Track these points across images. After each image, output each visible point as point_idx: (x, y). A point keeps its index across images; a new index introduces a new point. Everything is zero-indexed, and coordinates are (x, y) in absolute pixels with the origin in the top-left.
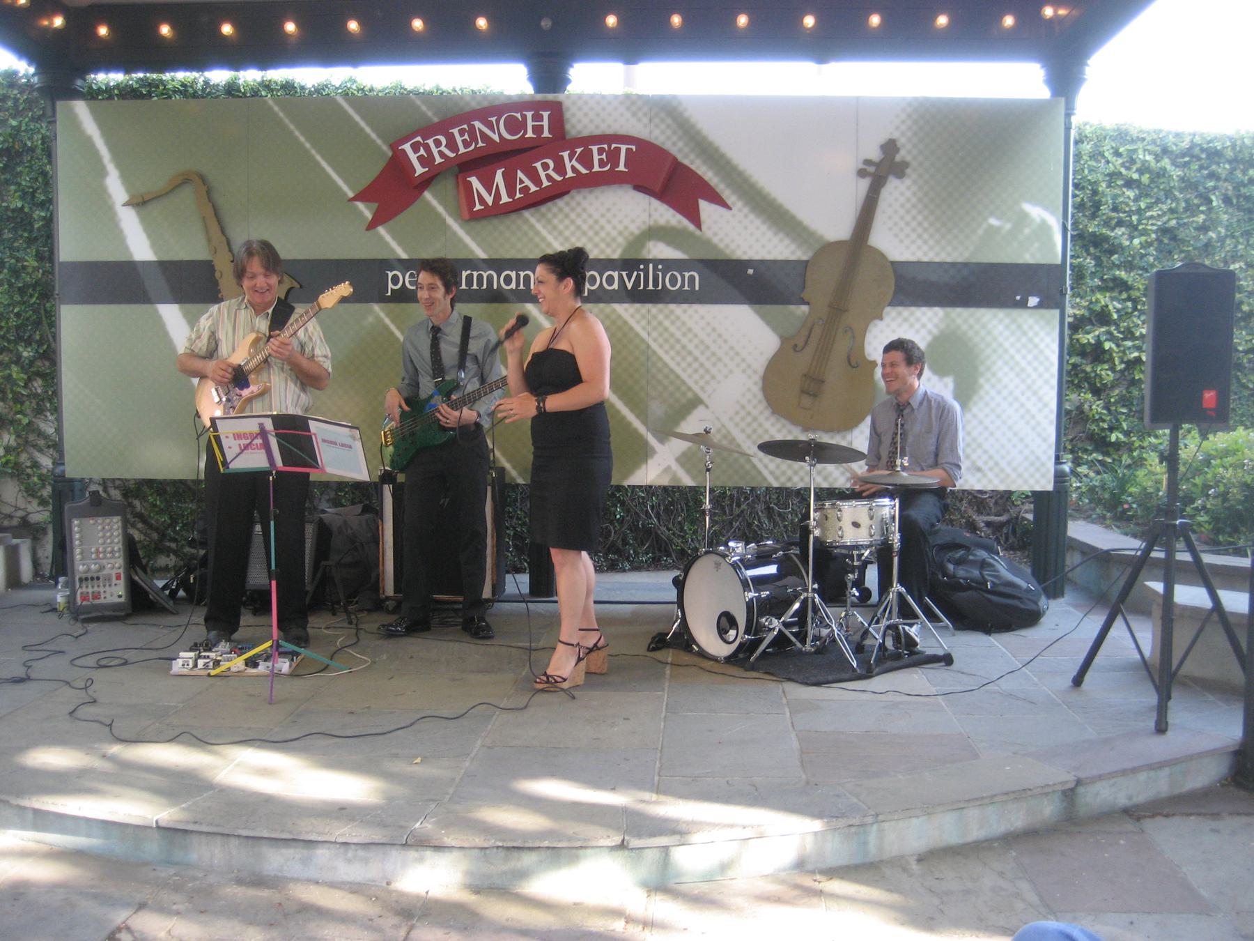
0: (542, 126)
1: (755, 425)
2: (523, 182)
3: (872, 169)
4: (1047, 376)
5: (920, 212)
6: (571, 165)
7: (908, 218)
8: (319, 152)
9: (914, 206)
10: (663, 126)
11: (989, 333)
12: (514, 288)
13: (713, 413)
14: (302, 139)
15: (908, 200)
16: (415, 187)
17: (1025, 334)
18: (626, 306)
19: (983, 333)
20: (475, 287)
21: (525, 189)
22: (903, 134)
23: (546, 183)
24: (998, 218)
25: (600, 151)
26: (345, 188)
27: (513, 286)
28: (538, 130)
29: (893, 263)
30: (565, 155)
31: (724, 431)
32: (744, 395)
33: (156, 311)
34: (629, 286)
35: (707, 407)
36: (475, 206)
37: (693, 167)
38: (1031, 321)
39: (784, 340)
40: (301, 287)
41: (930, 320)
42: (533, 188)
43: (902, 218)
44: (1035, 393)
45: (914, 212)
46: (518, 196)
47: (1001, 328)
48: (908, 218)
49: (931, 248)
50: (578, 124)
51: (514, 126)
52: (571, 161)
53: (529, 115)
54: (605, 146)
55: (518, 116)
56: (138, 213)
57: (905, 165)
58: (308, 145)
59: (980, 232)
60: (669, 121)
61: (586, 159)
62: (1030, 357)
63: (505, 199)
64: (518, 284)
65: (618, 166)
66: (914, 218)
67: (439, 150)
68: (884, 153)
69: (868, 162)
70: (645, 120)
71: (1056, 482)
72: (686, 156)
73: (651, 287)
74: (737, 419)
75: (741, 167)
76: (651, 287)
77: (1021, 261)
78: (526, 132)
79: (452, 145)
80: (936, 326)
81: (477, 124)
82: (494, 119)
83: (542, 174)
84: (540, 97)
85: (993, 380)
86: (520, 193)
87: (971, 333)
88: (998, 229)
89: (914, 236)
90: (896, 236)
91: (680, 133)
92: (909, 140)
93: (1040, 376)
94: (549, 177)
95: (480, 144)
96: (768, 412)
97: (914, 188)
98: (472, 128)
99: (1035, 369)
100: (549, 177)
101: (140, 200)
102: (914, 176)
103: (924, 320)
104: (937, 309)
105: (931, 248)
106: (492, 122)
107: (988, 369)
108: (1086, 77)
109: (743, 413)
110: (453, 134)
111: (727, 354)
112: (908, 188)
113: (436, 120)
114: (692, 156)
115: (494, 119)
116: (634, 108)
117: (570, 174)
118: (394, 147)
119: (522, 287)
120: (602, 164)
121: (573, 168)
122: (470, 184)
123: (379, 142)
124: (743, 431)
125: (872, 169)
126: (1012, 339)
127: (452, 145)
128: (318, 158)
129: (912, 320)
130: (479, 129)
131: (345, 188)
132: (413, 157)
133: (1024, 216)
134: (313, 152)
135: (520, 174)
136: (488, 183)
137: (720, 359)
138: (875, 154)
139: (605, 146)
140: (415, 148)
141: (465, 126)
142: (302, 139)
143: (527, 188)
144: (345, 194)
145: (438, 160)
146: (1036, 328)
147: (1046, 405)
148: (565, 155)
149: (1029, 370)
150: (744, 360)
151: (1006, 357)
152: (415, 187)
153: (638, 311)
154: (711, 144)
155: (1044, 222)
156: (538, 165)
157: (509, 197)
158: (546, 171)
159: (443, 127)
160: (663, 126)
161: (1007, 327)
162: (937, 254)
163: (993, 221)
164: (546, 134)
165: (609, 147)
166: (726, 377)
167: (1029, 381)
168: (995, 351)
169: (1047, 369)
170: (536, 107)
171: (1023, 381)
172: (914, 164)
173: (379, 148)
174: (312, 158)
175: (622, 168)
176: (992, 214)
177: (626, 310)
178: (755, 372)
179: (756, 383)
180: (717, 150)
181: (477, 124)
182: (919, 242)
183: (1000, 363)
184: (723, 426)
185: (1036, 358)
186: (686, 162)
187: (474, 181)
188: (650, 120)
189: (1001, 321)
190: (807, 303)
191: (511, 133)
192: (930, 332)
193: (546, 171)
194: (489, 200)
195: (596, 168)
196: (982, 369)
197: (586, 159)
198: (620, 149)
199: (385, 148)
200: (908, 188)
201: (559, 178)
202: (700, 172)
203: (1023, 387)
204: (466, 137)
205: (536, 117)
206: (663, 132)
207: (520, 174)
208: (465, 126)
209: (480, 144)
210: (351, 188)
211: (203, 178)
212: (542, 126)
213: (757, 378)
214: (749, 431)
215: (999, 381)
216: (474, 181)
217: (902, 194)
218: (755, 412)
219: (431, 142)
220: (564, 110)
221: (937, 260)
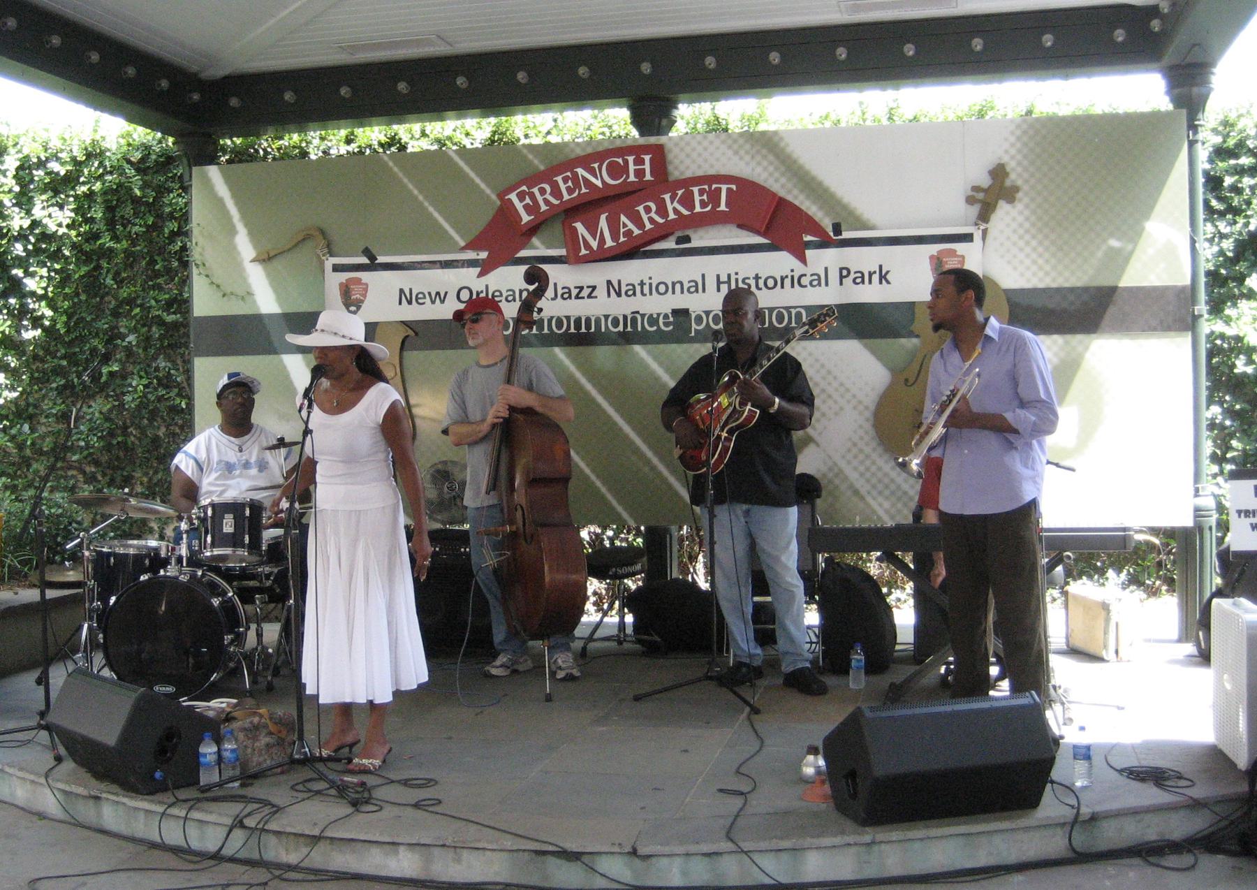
0: (644, 169)
1: (868, 463)
2: (627, 226)
3: (981, 196)
5: (1034, 237)
6: (673, 207)
7: (1021, 243)
9: (1027, 231)
10: (765, 163)
12: (622, 330)
13: (824, 451)
15: (1021, 225)
16: (523, 234)
20: (583, 330)
21: (628, 233)
22: (1013, 158)
23: (648, 226)
24: (1119, 239)
25: (701, 192)
28: (639, 173)
29: (1006, 291)
30: (667, 197)
31: (836, 470)
32: (855, 432)
33: (282, 361)
35: (818, 445)
37: (797, 203)
39: (895, 371)
40: (416, 334)
41: (1049, 348)
42: (637, 232)
43: (1014, 244)
45: (1027, 237)
46: (622, 239)
48: (1021, 243)
49: (1047, 274)
51: (615, 171)
52: (672, 203)
53: (631, 159)
55: (620, 160)
56: (265, 269)
57: (1016, 189)
58: (421, 198)
59: (1100, 254)
60: (771, 157)
61: (687, 201)
63: (609, 243)
65: (719, 206)
66: (1027, 243)
67: (544, 198)
68: (993, 179)
69: (976, 189)
70: (747, 158)
71: (1196, 516)
72: (789, 192)
74: (849, 456)
75: (846, 200)
78: (628, 177)
80: (1056, 354)
81: (580, 171)
82: (596, 165)
83: (645, 217)
84: (643, 141)
86: (624, 237)
89: (1028, 262)
90: (1009, 262)
91: (783, 169)
92: (1019, 164)
94: (651, 220)
95: (584, 190)
96: (880, 450)
97: (1027, 213)
98: (576, 175)
100: (651, 220)
101: (266, 256)
102: (1026, 200)
104: (1056, 337)
105: (1047, 274)
106: (594, 168)
108: (1212, 86)
109: (855, 451)
110: (556, 181)
111: (836, 390)
112: (1021, 213)
113: (542, 168)
114: (796, 192)
115: (596, 165)
116: (735, 147)
117: (672, 216)
118: (502, 195)
119: (629, 329)
120: (703, 204)
121: (675, 210)
122: (575, 229)
123: (488, 191)
124: (855, 469)
125: (981, 196)
127: (556, 193)
128: (431, 209)
130: (582, 176)
132: (519, 206)
134: (426, 204)
135: (623, 218)
136: (592, 228)
137: (830, 396)
138: (985, 181)
140: (521, 197)
141: (569, 174)
144: (456, 243)
145: (544, 208)
148: (667, 197)
150: (854, 396)
152: (523, 234)
154: (813, 179)
156: (641, 209)
158: (649, 214)
159: (547, 176)
162: (1054, 280)
163: (1114, 243)
164: (648, 177)
165: (710, 187)
166: (836, 414)
170: (637, 151)
172: (1025, 188)
173: (488, 197)
175: (723, 207)
176: (1112, 235)
178: (867, 408)
179: (867, 420)
180: (820, 184)
182: (1034, 268)
184: (835, 464)
186: (790, 198)
187: (580, 227)
188: (753, 157)
190: (917, 336)
193: (649, 214)
194: (594, 244)
195: (698, 209)
198: (720, 188)
199: (494, 197)
201: (661, 221)
202: (803, 208)
204: (570, 184)
205: (639, 161)
206: (765, 169)
207: (623, 218)
208: (569, 174)
209: (584, 190)
210: (462, 237)
211: (323, 233)
212: (644, 169)
213: (868, 414)
214: (862, 468)
216: (580, 227)
217: (1014, 219)
218: (867, 450)
219: (536, 190)
220: (666, 151)
221: (1054, 285)
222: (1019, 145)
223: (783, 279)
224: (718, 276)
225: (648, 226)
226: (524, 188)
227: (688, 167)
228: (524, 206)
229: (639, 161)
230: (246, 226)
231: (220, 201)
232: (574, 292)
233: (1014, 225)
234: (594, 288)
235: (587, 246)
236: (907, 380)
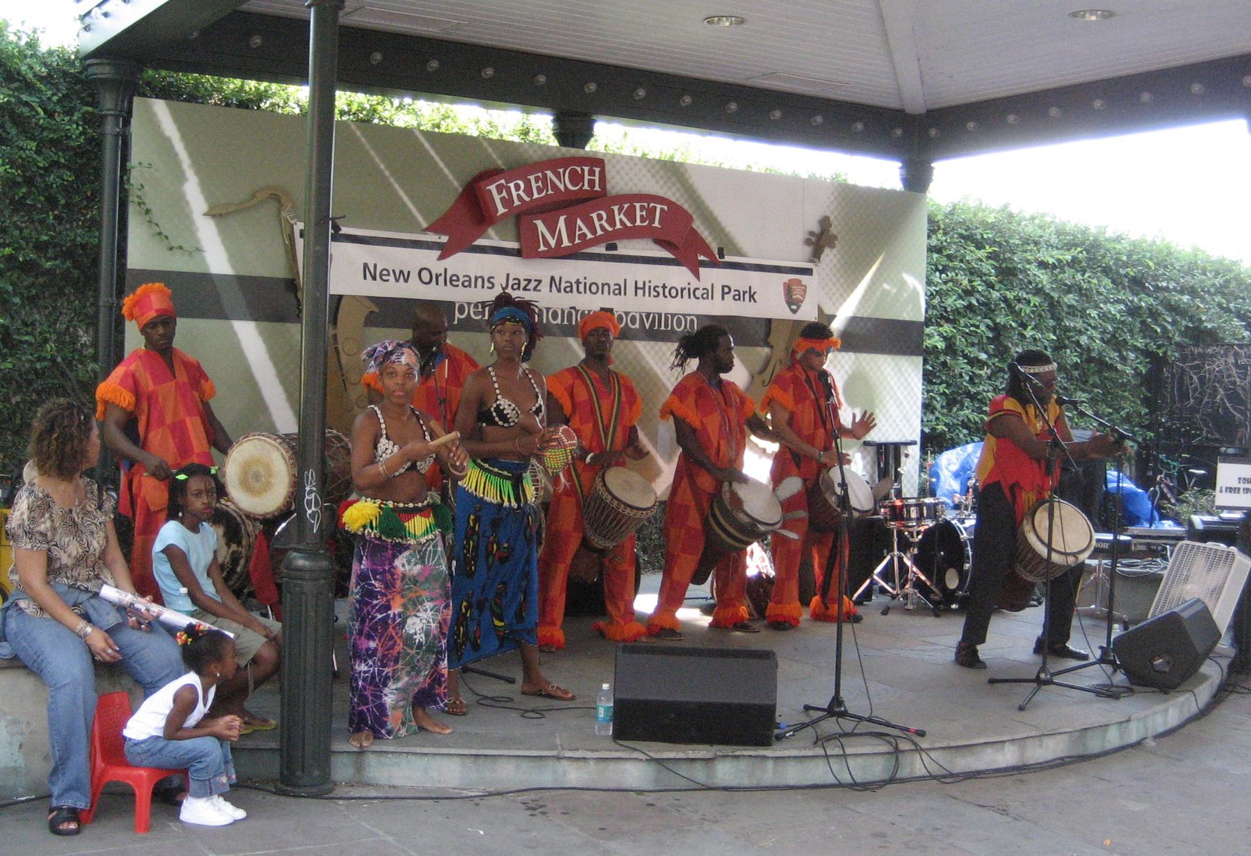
4: (915, 408)
8: (397, 180)
10: (674, 189)
11: (882, 373)
14: (382, 166)
15: (835, 266)
17: (902, 375)
18: (643, 343)
19: (878, 373)
22: (832, 213)
23: (600, 232)
24: (888, 284)
25: (642, 208)
26: (420, 219)
27: (559, 321)
28: (592, 183)
30: (616, 208)
33: (232, 327)
34: (647, 326)
36: (539, 247)
38: (906, 365)
41: (847, 362)
42: (590, 236)
44: (908, 421)
46: (577, 241)
47: (889, 369)
50: (618, 183)
51: (576, 178)
53: (586, 169)
54: (646, 204)
55: (579, 169)
56: (218, 225)
57: (835, 237)
59: (878, 294)
60: (678, 185)
61: (631, 215)
62: (905, 393)
63: (566, 243)
64: (563, 320)
69: (811, 233)
73: (663, 328)
75: (727, 229)
76: (663, 328)
77: (901, 319)
78: (583, 185)
79: (529, 191)
80: (850, 367)
83: (597, 224)
85: (884, 411)
87: (871, 374)
88: (889, 292)
91: (686, 196)
93: (911, 408)
94: (602, 227)
95: (550, 192)
97: (839, 256)
98: (545, 176)
99: (908, 402)
100: (602, 227)
103: (843, 362)
104: (851, 354)
107: (881, 401)
115: (561, 170)
117: (618, 226)
119: (565, 322)
121: (621, 220)
122: (536, 226)
123: (451, 177)
126: (896, 379)
127: (529, 191)
128: (396, 186)
129: (836, 362)
131: (420, 219)
133: (904, 283)
134: (392, 180)
135: (579, 222)
136: (552, 228)
138: (816, 228)
139: (646, 204)
141: (540, 174)
142: (382, 166)
143: (584, 235)
144: (419, 224)
145: (517, 203)
146: (909, 370)
147: (914, 431)
148: (616, 208)
149: (905, 403)
151: (892, 393)
153: (653, 348)
155: (915, 288)
156: (594, 215)
157: (570, 241)
160: (674, 189)
161: (892, 369)
163: (886, 286)
164: (597, 188)
167: (905, 412)
168: (885, 388)
169: (915, 403)
171: (901, 412)
172: (839, 238)
174: (390, 185)
175: (656, 224)
176: (885, 280)
177: (644, 347)
181: (549, 173)
183: (888, 398)
185: (909, 393)
187: (540, 225)
189: (889, 365)
191: (574, 183)
192: (846, 372)
193: (600, 222)
194: (553, 243)
196: (877, 402)
197: (631, 215)
199: (456, 183)
200: (835, 256)
201: (610, 229)
203: (901, 417)
204: (540, 184)
205: (592, 173)
206: (674, 194)
207: (579, 222)
208: (540, 174)
209: (550, 192)
210: (425, 218)
215: (887, 411)
216: (540, 225)
217: (831, 261)
219: (512, 185)
222: (836, 203)
223: (682, 290)
224: (636, 282)
225: (600, 232)
226: (503, 181)
227: (617, 183)
228: (501, 199)
229: (592, 173)
230: (197, 173)
231: (167, 141)
232: (523, 284)
233: (831, 265)
234: (540, 281)
235: (546, 243)
236: (764, 382)
